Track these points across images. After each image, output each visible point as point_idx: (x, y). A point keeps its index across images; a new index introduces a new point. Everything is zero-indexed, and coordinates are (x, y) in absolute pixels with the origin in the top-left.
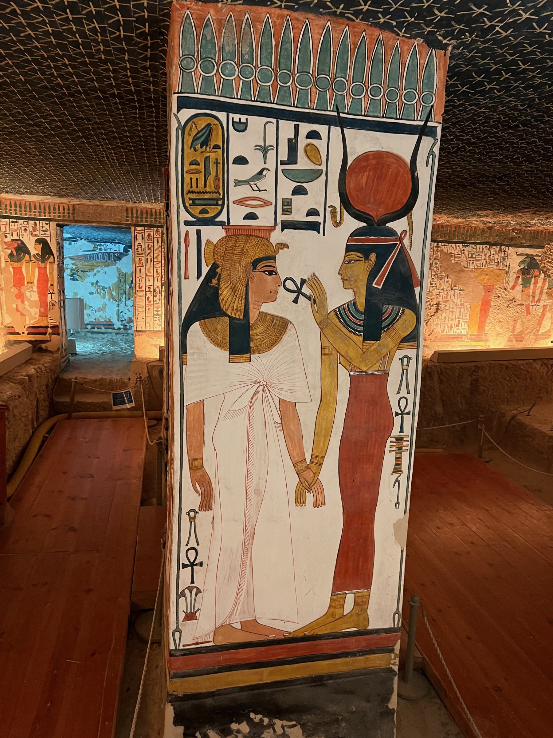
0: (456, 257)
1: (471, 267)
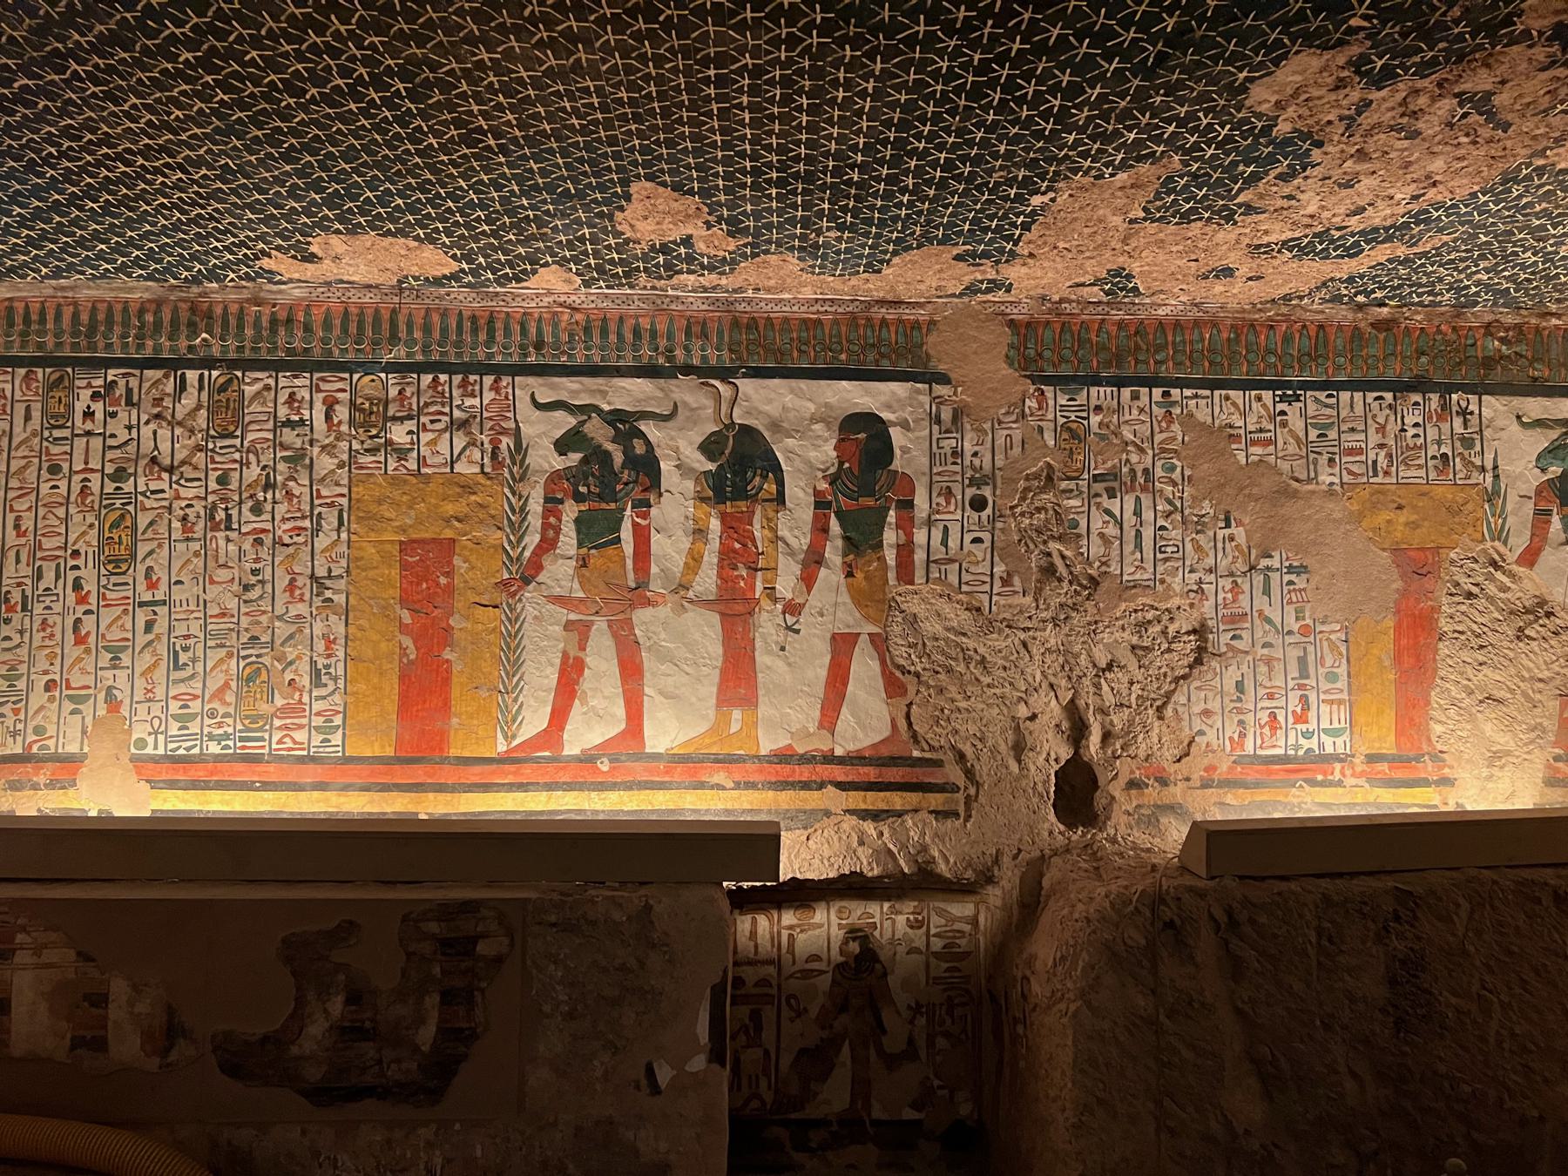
0: (1254, 443)
1: (1325, 478)
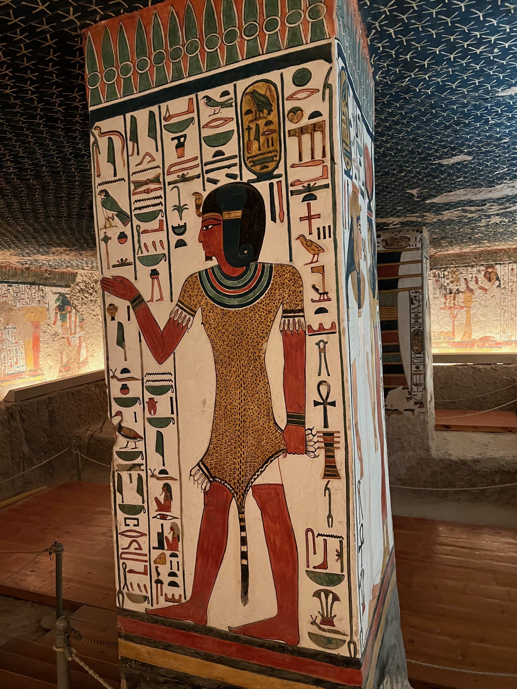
1: (18, 306)
